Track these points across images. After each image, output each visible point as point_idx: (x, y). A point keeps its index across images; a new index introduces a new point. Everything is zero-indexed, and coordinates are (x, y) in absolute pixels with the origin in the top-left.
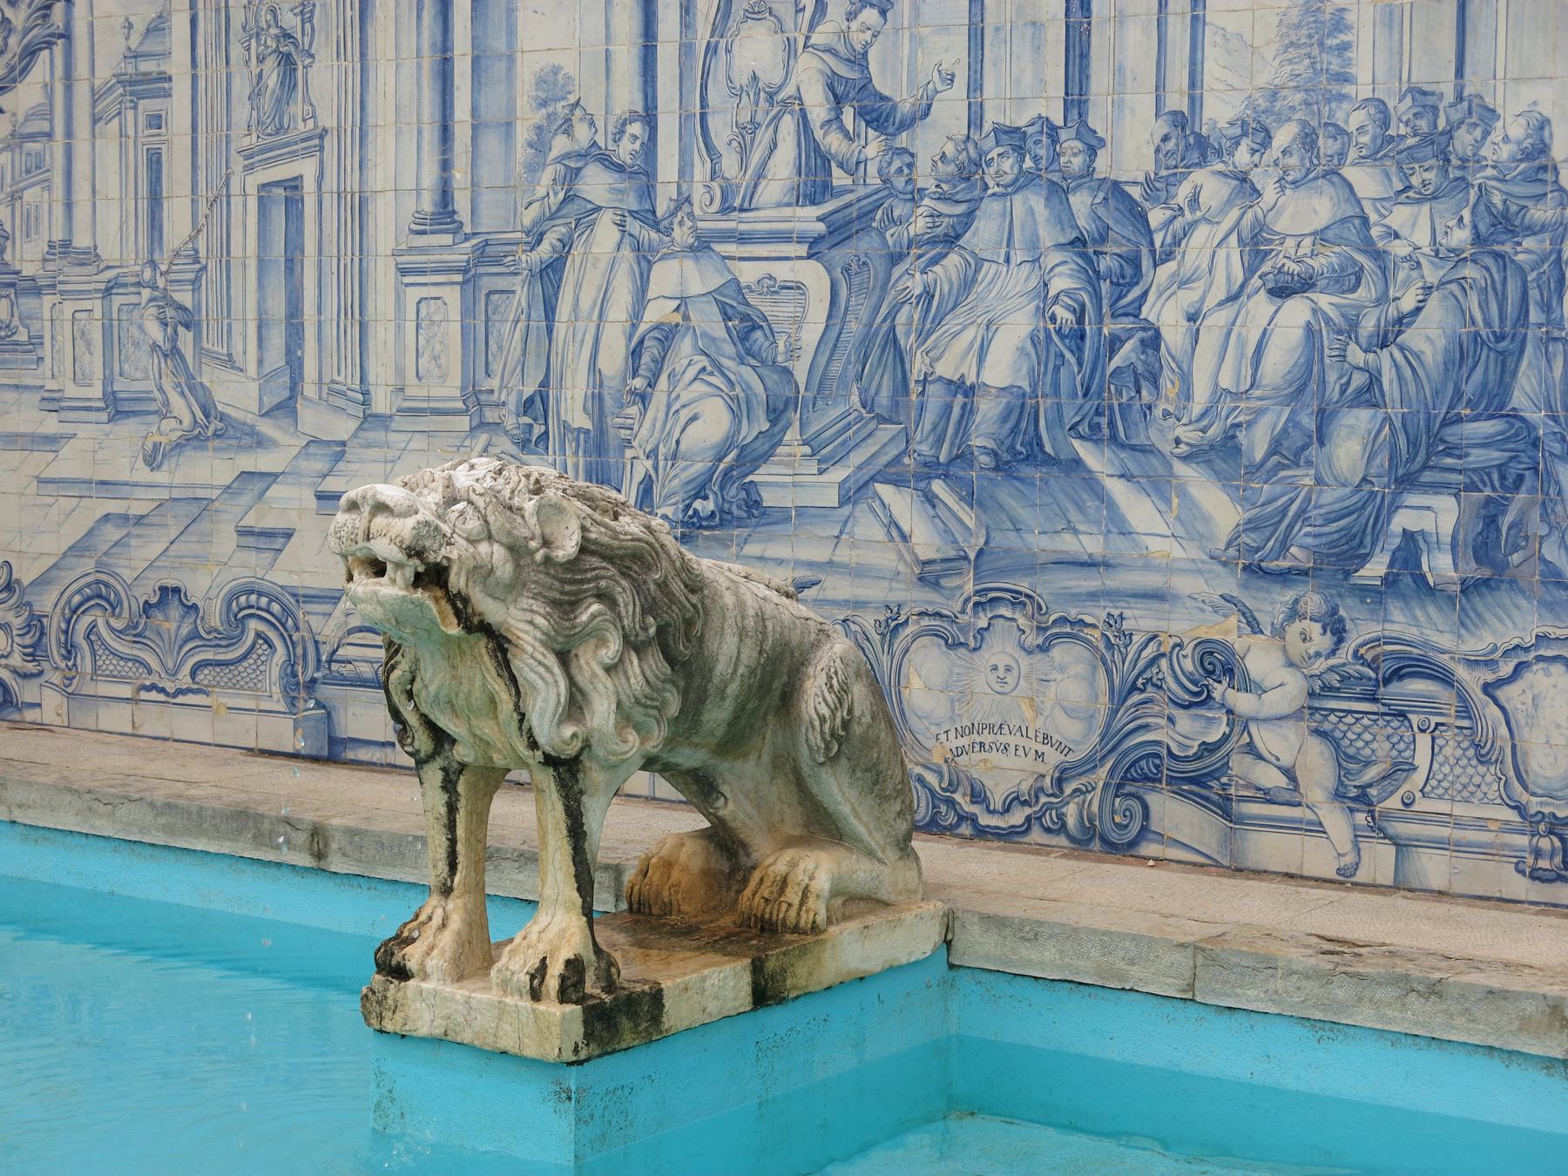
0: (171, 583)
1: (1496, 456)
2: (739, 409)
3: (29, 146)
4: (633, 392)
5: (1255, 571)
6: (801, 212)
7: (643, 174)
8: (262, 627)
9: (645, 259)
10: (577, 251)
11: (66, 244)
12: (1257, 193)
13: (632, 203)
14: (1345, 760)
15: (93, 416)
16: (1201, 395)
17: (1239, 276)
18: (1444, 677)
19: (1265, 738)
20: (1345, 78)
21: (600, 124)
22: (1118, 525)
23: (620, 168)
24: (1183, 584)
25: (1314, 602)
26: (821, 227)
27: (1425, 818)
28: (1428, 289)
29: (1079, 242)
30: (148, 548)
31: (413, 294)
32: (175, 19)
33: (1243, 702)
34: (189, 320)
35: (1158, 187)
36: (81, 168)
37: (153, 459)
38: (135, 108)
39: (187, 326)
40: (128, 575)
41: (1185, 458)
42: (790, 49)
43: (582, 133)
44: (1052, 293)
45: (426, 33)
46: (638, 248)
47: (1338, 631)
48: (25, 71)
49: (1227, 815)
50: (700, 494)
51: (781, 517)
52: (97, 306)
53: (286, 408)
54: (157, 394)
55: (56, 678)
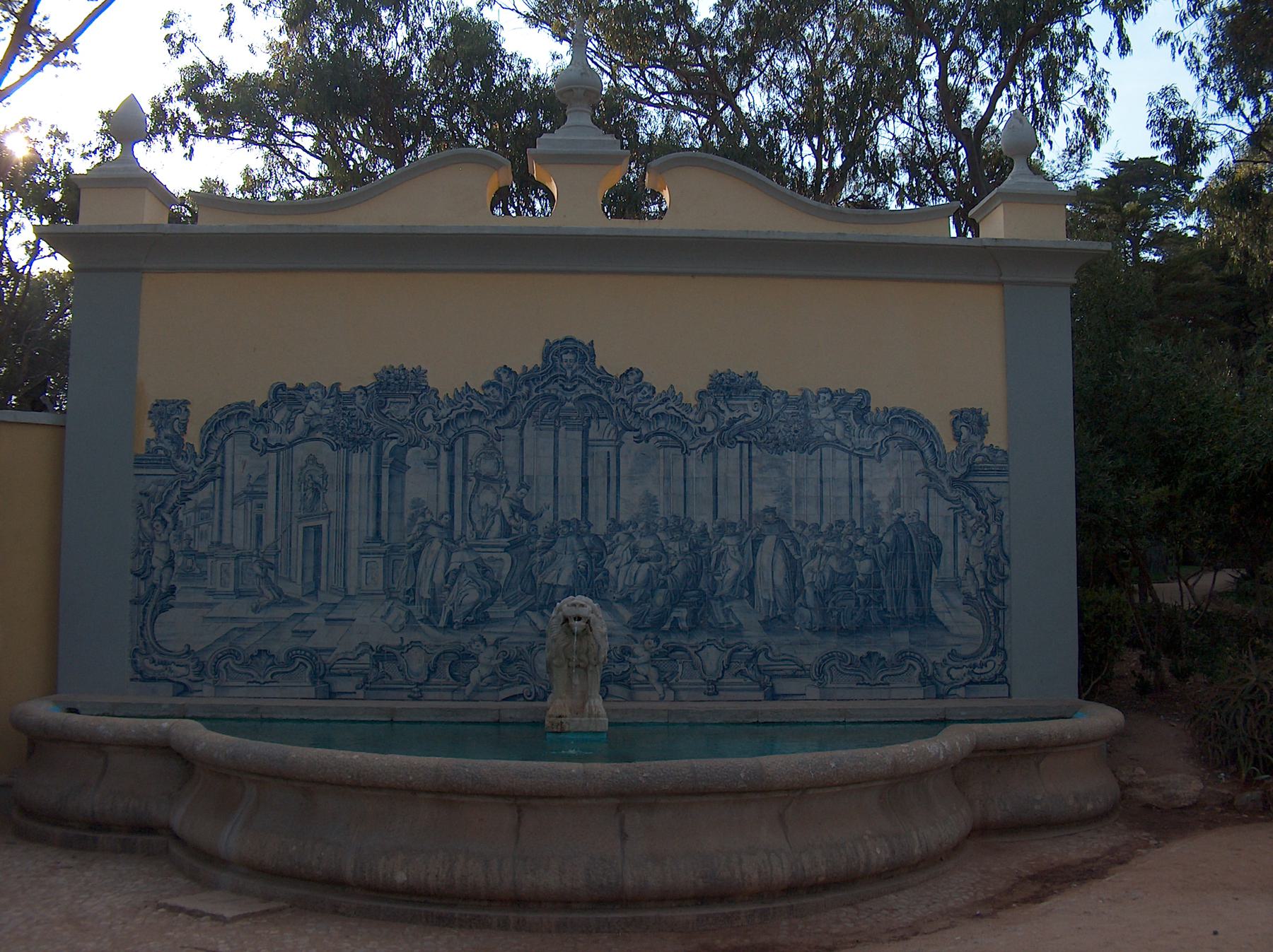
0: (263, 649)
1: (696, 599)
2: (482, 592)
3: (202, 511)
4: (446, 588)
5: (637, 629)
6: (502, 540)
8: (302, 660)
9: (450, 553)
10: (425, 550)
11: (219, 543)
12: (635, 538)
13: (446, 536)
14: (660, 672)
15: (230, 597)
16: (620, 586)
17: (630, 558)
18: (686, 651)
19: (640, 669)
20: (657, 512)
21: (434, 512)
23: (442, 527)
25: (651, 635)
26: (509, 544)
27: (680, 684)
28: (679, 561)
29: (585, 549)
31: (365, 560)
32: (270, 476)
33: (633, 660)
35: (607, 537)
36: (227, 519)
37: (256, 610)
38: (251, 501)
39: (272, 569)
40: (244, 647)
41: (616, 602)
42: (498, 496)
43: (428, 517)
44: (579, 561)
45: (371, 486)
46: (447, 548)
47: (657, 641)
48: (202, 488)
49: (630, 688)
50: (469, 615)
52: (233, 562)
53: (314, 593)
54: (258, 590)
55: (211, 681)
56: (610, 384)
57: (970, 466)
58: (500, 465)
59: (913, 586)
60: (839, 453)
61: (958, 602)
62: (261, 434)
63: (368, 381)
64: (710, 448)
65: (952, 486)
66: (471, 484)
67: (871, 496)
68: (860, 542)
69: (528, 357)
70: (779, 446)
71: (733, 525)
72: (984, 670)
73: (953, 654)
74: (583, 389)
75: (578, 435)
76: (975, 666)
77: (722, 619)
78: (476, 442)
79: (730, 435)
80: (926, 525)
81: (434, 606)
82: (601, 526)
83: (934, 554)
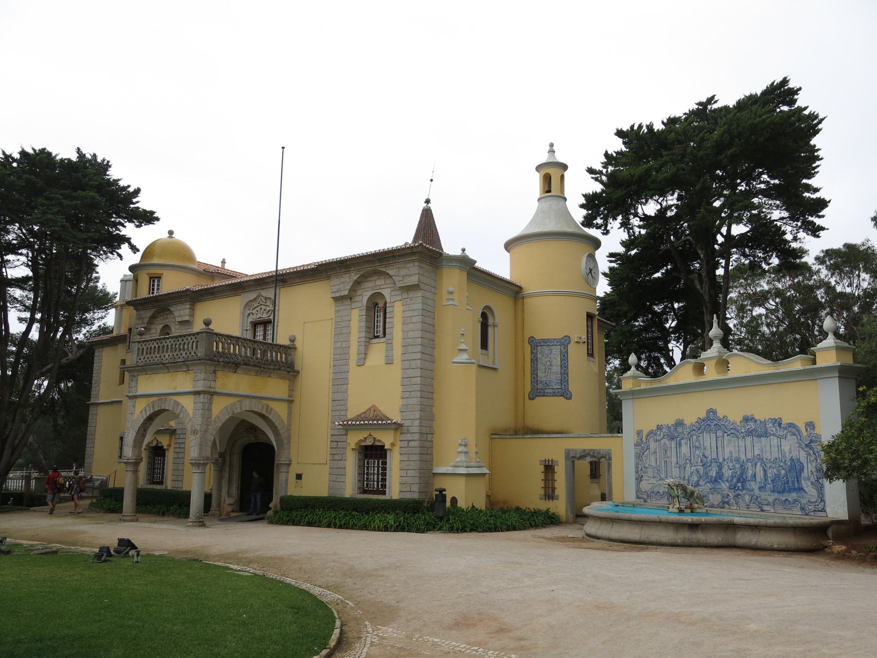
2: (698, 478)
7: (691, 460)
9: (691, 466)
14: (736, 501)
19: (731, 500)
22: (722, 486)
24: (726, 490)
30: (656, 488)
34: (659, 471)
37: (657, 481)
51: (700, 485)
53: (666, 477)
56: (720, 420)
57: (811, 440)
58: (699, 444)
59: (797, 478)
60: (775, 437)
61: (809, 484)
62: (655, 438)
63: (673, 423)
64: (744, 437)
65: (806, 447)
66: (694, 449)
67: (784, 450)
68: (782, 465)
69: (703, 415)
70: (759, 436)
71: (750, 459)
72: (819, 507)
73: (809, 501)
74: (715, 422)
75: (714, 435)
76: (816, 505)
77: (749, 487)
78: (695, 437)
79: (750, 433)
80: (799, 459)
81: (688, 480)
82: (721, 461)
83: (802, 470)
